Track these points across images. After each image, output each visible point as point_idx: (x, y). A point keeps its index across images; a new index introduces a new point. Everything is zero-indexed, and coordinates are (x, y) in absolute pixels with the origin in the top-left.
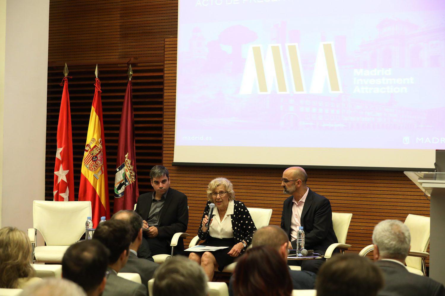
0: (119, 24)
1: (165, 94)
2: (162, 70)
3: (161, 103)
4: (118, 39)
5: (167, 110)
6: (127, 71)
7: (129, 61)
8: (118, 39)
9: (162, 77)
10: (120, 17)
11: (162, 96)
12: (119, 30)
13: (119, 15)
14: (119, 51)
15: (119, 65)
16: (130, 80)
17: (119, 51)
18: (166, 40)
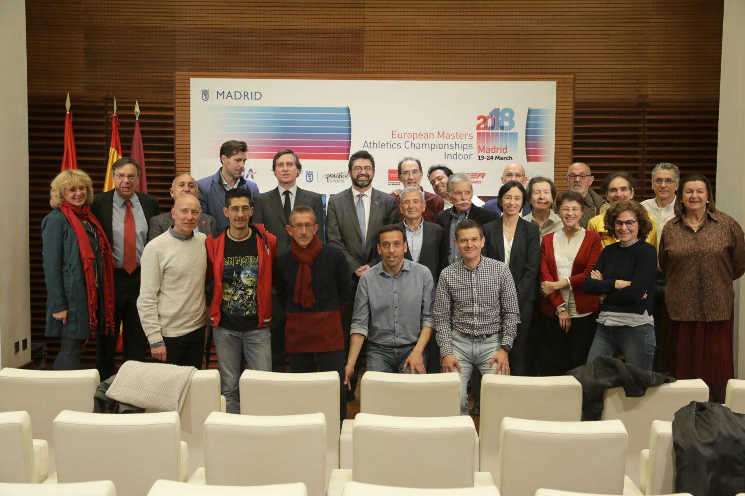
0: (83, 47)
1: (177, 139)
2: (172, 109)
3: (172, 149)
4: (83, 66)
5: (180, 158)
6: (133, 109)
7: (107, 96)
8: (83, 66)
9: (172, 117)
10: (85, 37)
11: (172, 141)
12: (83, 54)
13: (82, 36)
14: (86, 81)
15: (86, 99)
16: (137, 119)
17: (86, 81)
18: (177, 73)
